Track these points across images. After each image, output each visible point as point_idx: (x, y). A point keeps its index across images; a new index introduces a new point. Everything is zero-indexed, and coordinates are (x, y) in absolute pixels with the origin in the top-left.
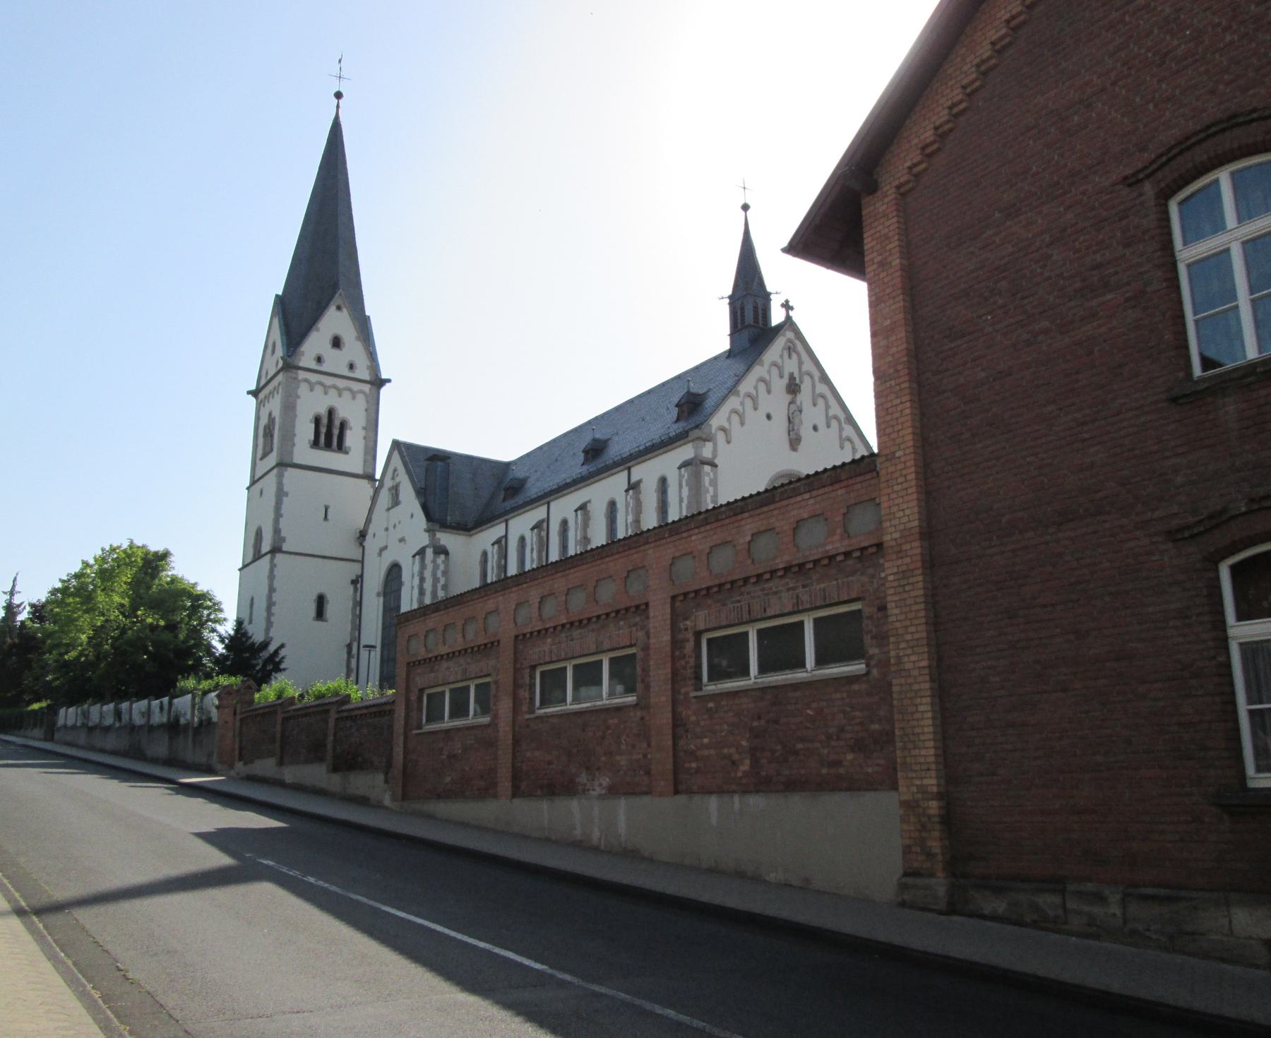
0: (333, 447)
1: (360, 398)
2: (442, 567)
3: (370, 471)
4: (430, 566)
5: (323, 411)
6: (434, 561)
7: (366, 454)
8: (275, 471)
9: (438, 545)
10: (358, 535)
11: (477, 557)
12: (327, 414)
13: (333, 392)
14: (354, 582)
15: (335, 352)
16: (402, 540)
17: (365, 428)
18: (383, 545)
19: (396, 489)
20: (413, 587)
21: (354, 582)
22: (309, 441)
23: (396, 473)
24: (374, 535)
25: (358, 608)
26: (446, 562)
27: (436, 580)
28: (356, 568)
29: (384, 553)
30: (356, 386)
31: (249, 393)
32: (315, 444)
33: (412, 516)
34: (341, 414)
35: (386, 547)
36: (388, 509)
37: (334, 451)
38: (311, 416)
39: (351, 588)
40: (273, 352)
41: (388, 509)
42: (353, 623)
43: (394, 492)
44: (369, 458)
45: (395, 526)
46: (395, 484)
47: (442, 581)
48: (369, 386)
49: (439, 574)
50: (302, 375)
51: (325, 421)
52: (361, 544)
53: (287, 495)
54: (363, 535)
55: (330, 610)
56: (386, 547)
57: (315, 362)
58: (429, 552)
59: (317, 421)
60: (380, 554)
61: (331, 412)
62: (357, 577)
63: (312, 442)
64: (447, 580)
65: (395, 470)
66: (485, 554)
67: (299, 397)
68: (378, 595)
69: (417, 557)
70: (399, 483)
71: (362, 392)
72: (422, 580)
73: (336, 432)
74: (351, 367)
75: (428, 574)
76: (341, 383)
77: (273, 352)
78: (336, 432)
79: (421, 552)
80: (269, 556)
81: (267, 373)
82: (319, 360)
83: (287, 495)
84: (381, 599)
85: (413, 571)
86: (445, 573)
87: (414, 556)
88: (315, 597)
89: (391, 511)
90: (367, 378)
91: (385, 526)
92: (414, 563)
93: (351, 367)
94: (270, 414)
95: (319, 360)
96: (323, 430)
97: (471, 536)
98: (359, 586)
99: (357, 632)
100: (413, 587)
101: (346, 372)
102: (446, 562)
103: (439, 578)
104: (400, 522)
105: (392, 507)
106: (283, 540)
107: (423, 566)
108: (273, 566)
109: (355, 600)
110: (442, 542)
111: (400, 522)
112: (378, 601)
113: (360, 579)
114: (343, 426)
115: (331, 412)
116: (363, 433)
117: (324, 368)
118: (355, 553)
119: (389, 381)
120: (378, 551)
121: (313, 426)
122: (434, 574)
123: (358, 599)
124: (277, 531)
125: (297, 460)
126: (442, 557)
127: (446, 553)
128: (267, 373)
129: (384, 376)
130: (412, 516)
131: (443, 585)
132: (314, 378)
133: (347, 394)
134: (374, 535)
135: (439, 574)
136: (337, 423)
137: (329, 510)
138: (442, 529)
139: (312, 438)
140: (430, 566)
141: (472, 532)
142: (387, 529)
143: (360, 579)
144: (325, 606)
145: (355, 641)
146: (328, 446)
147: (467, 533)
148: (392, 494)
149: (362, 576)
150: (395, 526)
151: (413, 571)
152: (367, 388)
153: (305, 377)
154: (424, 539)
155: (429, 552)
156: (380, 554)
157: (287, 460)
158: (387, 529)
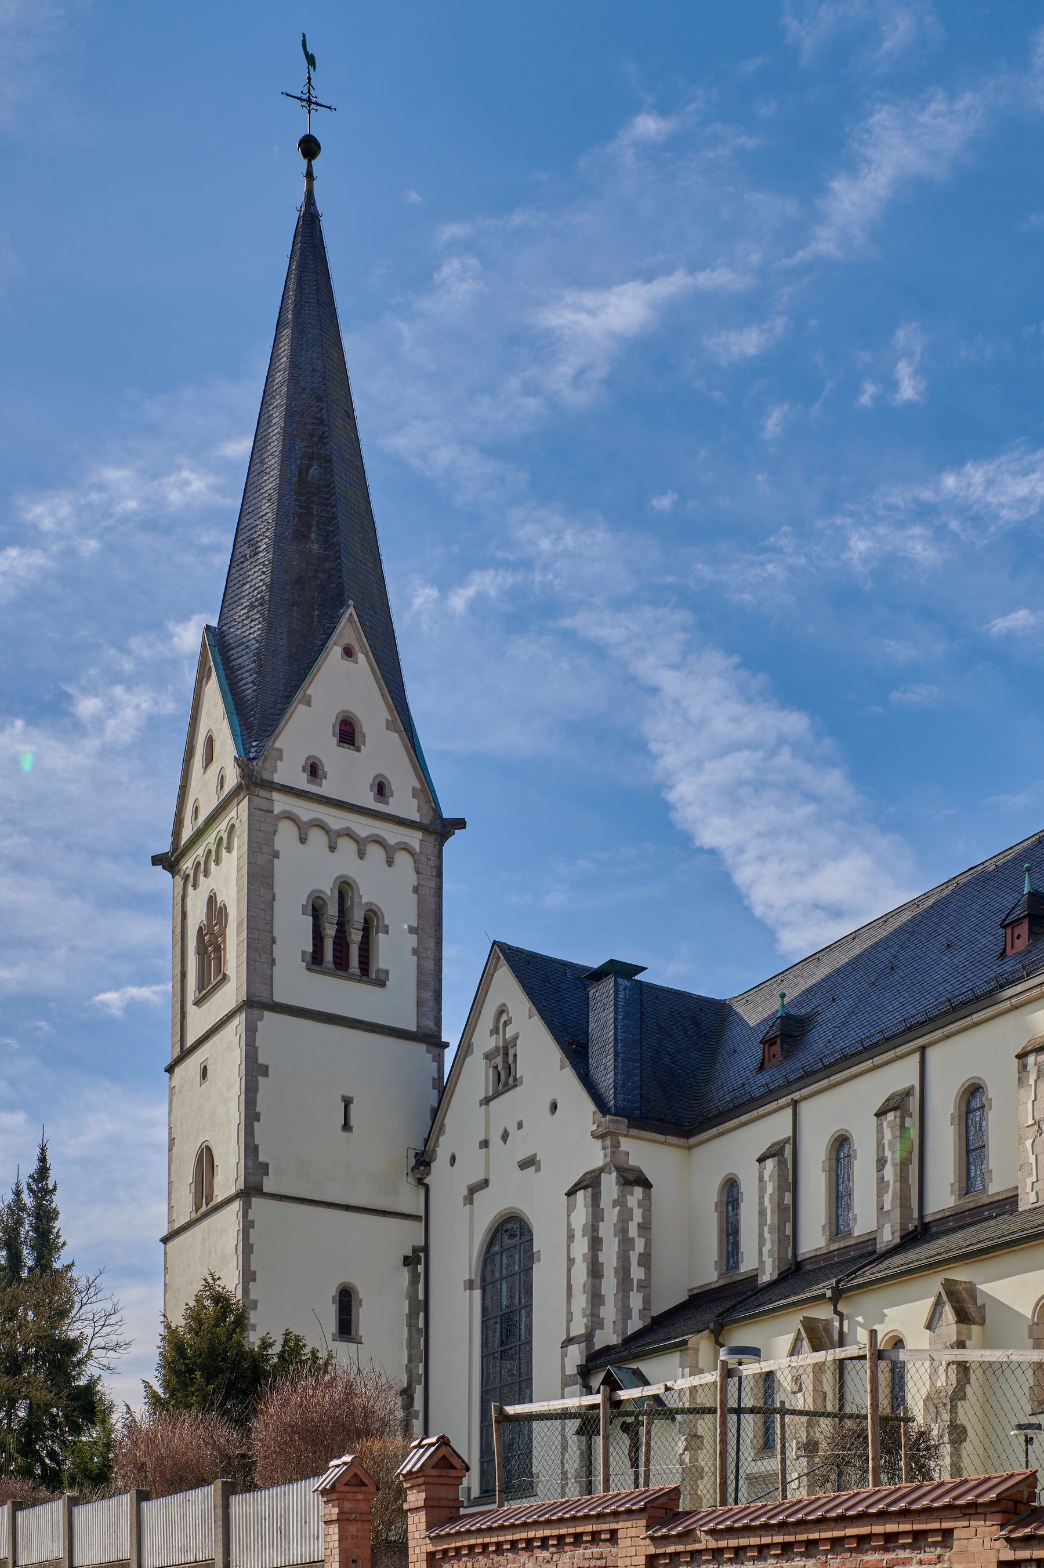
0: (351, 970)
1: (403, 860)
2: (638, 1216)
3: (430, 1024)
4: (611, 1216)
5: (327, 887)
6: (620, 1202)
7: (421, 985)
8: (240, 1021)
9: (625, 1166)
10: (412, 1162)
11: (711, 1194)
12: (337, 895)
14: (409, 1261)
16: (529, 1163)
17: (412, 930)
18: (478, 1177)
19: (506, 1054)
20: (571, 1261)
21: (409, 1261)
23: (504, 1018)
24: (453, 1159)
25: (422, 1315)
26: (646, 1204)
27: (626, 1244)
28: (410, 1234)
29: (476, 1196)
30: (393, 834)
32: (316, 960)
33: (554, 1107)
34: (367, 894)
35: (486, 1183)
36: (487, 1101)
37: (352, 978)
39: (405, 1274)
40: (209, 759)
41: (487, 1101)
42: (411, 1345)
43: (499, 1060)
44: (428, 995)
45: (505, 1136)
46: (501, 1044)
47: (640, 1245)
48: (419, 835)
49: (633, 1231)
51: (332, 910)
52: (420, 1181)
53: (264, 1071)
54: (423, 1162)
55: (365, 1319)
56: (486, 1183)
57: (305, 776)
58: (610, 1184)
59: (316, 910)
60: (469, 1200)
62: (415, 1250)
63: (309, 958)
64: (648, 1244)
65: (502, 1011)
66: (731, 1189)
67: (276, 855)
68: (470, 1285)
69: (580, 1194)
70: (516, 1037)
71: (406, 848)
72: (596, 1244)
73: (355, 936)
74: (381, 789)
75: (607, 1230)
76: (364, 827)
77: (209, 759)
78: (355, 936)
79: (590, 1182)
80: (236, 1206)
81: (196, 810)
83: (264, 1071)
84: (477, 1293)
85: (569, 1224)
86: (645, 1228)
87: (570, 1193)
88: (333, 1292)
89: (492, 1103)
90: (416, 817)
91: (482, 1138)
92: (570, 1209)
93: (381, 789)
94: (212, 900)
96: (330, 931)
97: (690, 1148)
98: (421, 1268)
99: (421, 1366)
100: (571, 1261)
102: (646, 1204)
103: (633, 1239)
104: (520, 1126)
105: (497, 1095)
106: (264, 1168)
107: (596, 1215)
108: (247, 1225)
109: (412, 1297)
110: (633, 1162)
111: (520, 1126)
112: (471, 1296)
113: (422, 1255)
116: (413, 940)
118: (409, 1200)
119: (461, 824)
120: (465, 1193)
122: (622, 1230)
123: (421, 1297)
124: (251, 1150)
125: (279, 997)
126: (638, 1191)
127: (646, 1184)
128: (196, 810)
129: (448, 812)
130: (554, 1107)
131: (640, 1254)
134: (453, 1159)
135: (633, 1231)
136: (358, 917)
137: (353, 1108)
138: (634, 1132)
139: (310, 949)
140: (611, 1216)
141: (692, 1141)
142: (485, 1144)
143: (422, 1255)
144: (353, 1311)
145: (419, 1383)
146: (341, 964)
147: (682, 1141)
148: (496, 1067)
149: (426, 1249)
150: (505, 1136)
151: (569, 1224)
152: (414, 839)
153: (288, 808)
154: (595, 1156)
155: (610, 1184)
156: (469, 1200)
157: (264, 997)
158: (485, 1144)
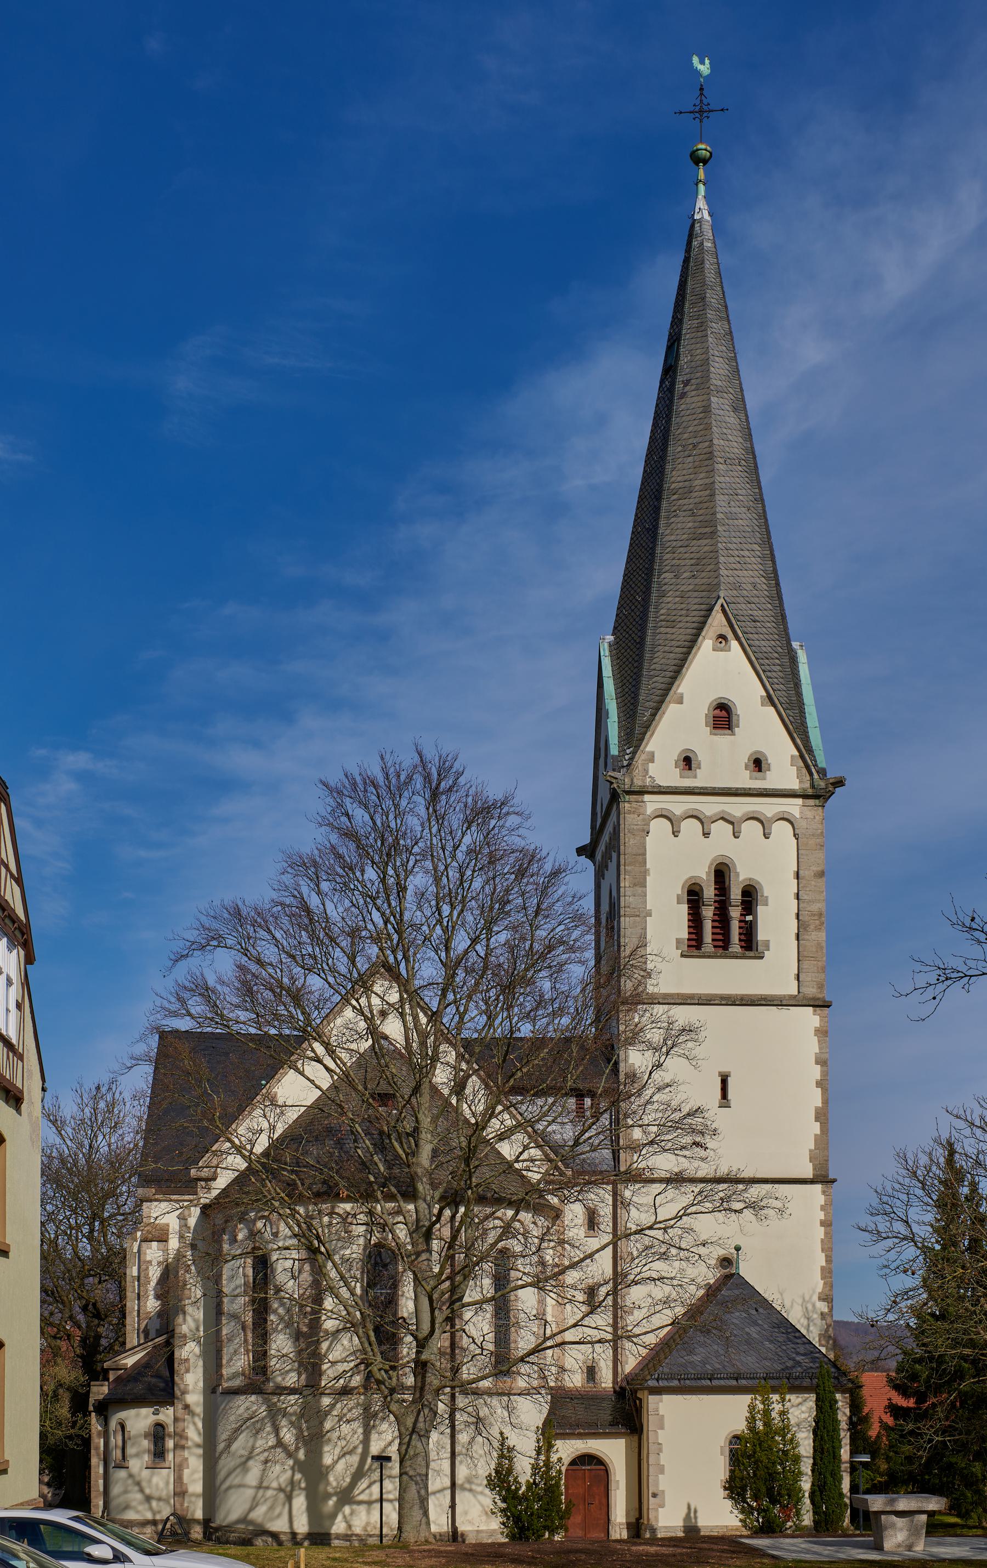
1: (782, 830)
5: (703, 873)
13: (721, 829)
15: (723, 740)
22: (678, 941)
30: (769, 807)
31: (580, 851)
32: (695, 944)
38: (678, 889)
50: (652, 803)
51: (709, 892)
59: (694, 896)
61: (721, 874)
73: (735, 913)
74: (758, 764)
76: (737, 807)
82: (688, 762)
93: (758, 764)
95: (688, 762)
96: (708, 913)
101: (745, 780)
114: (750, 896)
115: (721, 874)
117: (700, 781)
121: (684, 908)
132: (678, 805)
133: (751, 829)
136: (736, 894)
139: (684, 934)
